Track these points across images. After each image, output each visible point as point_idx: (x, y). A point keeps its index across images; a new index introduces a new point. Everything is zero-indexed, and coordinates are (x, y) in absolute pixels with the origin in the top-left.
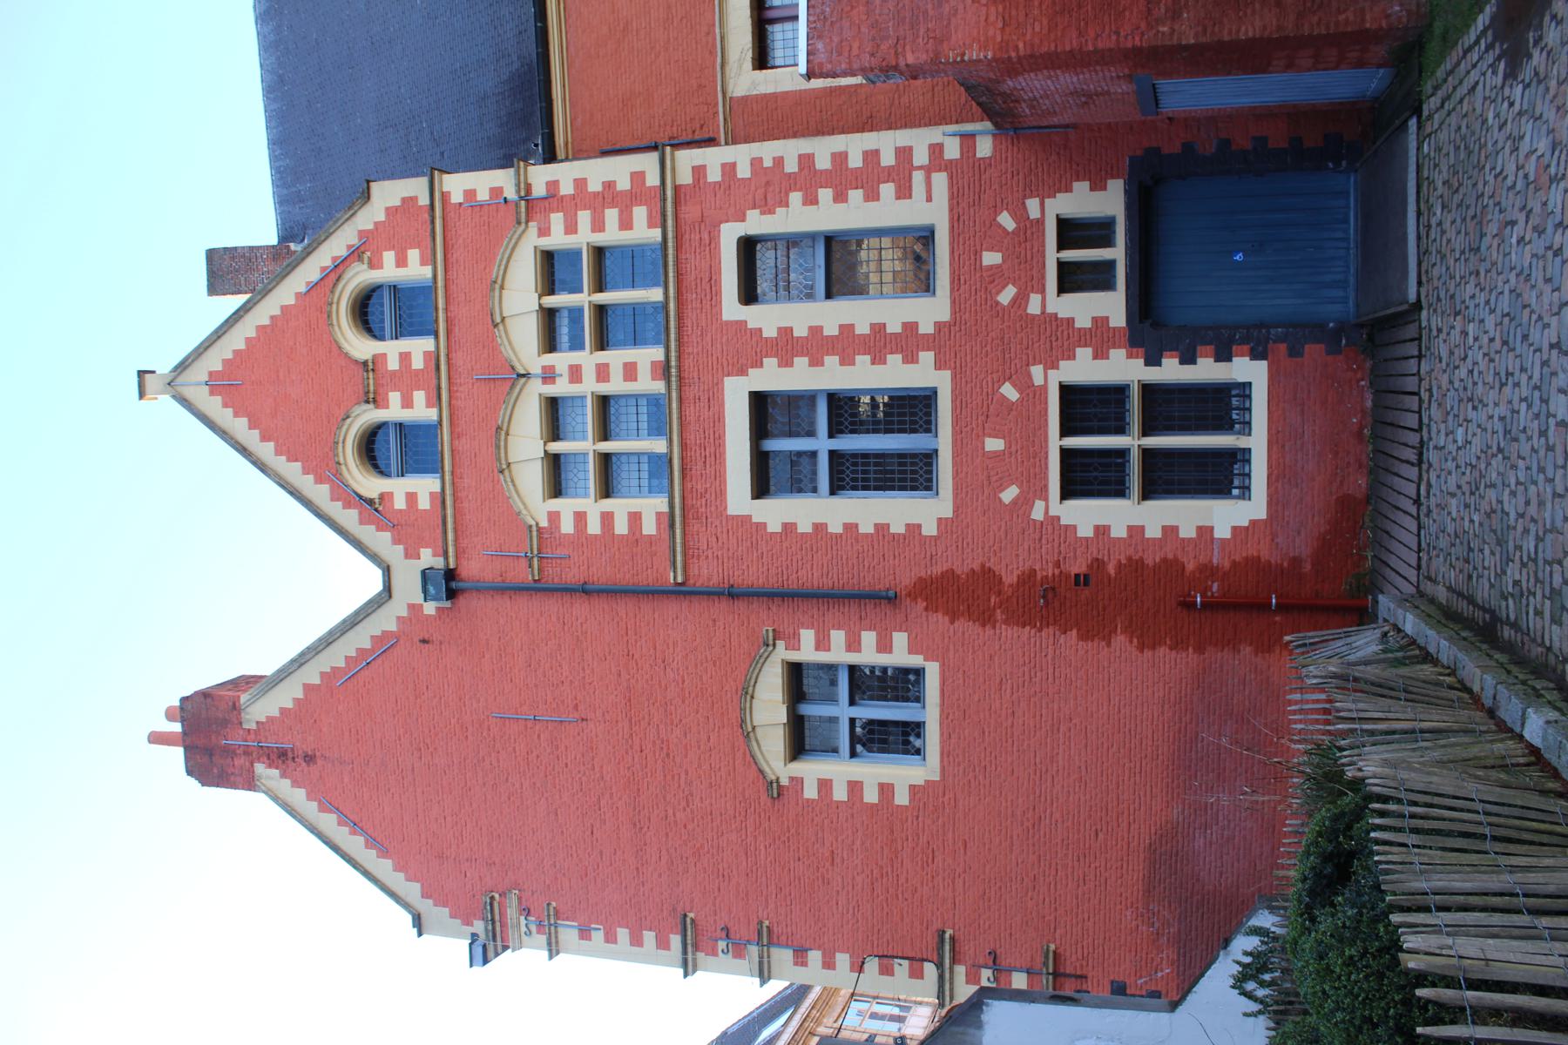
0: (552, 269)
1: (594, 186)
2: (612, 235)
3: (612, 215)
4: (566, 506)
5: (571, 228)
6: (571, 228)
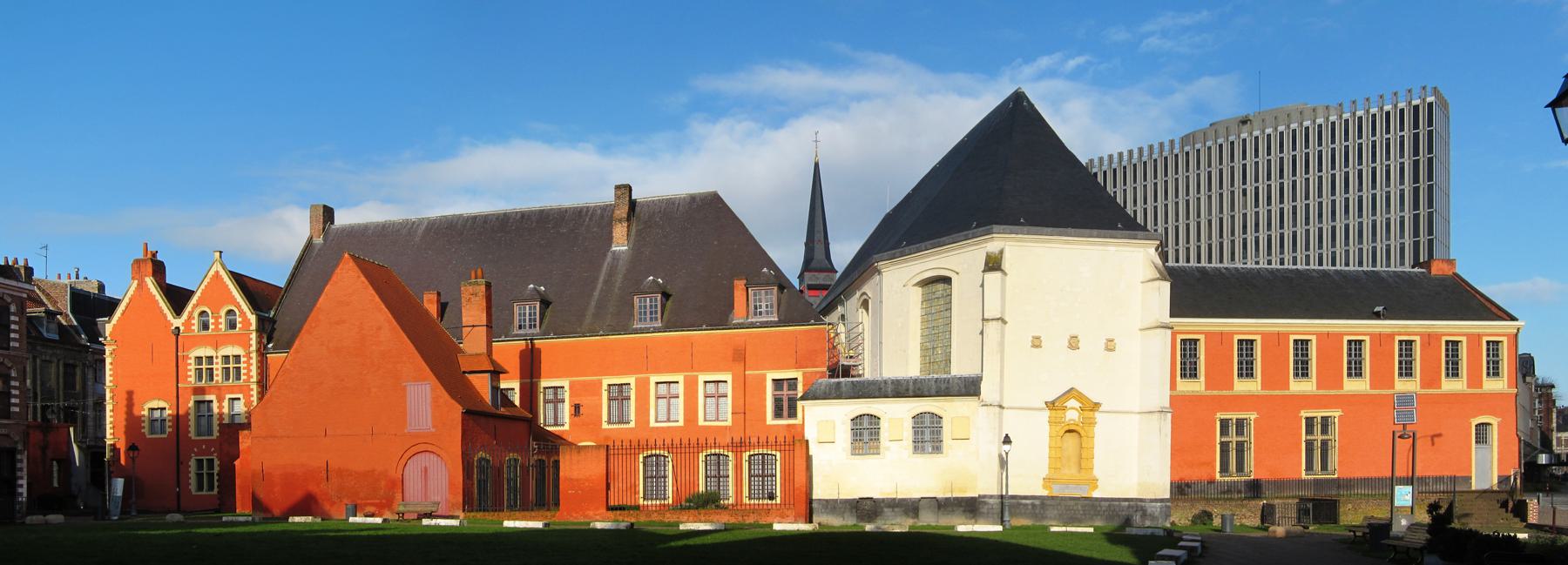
0: (237, 358)
1: (251, 368)
2: (243, 371)
3: (245, 371)
4: (192, 361)
5: (244, 362)
6: (244, 362)
